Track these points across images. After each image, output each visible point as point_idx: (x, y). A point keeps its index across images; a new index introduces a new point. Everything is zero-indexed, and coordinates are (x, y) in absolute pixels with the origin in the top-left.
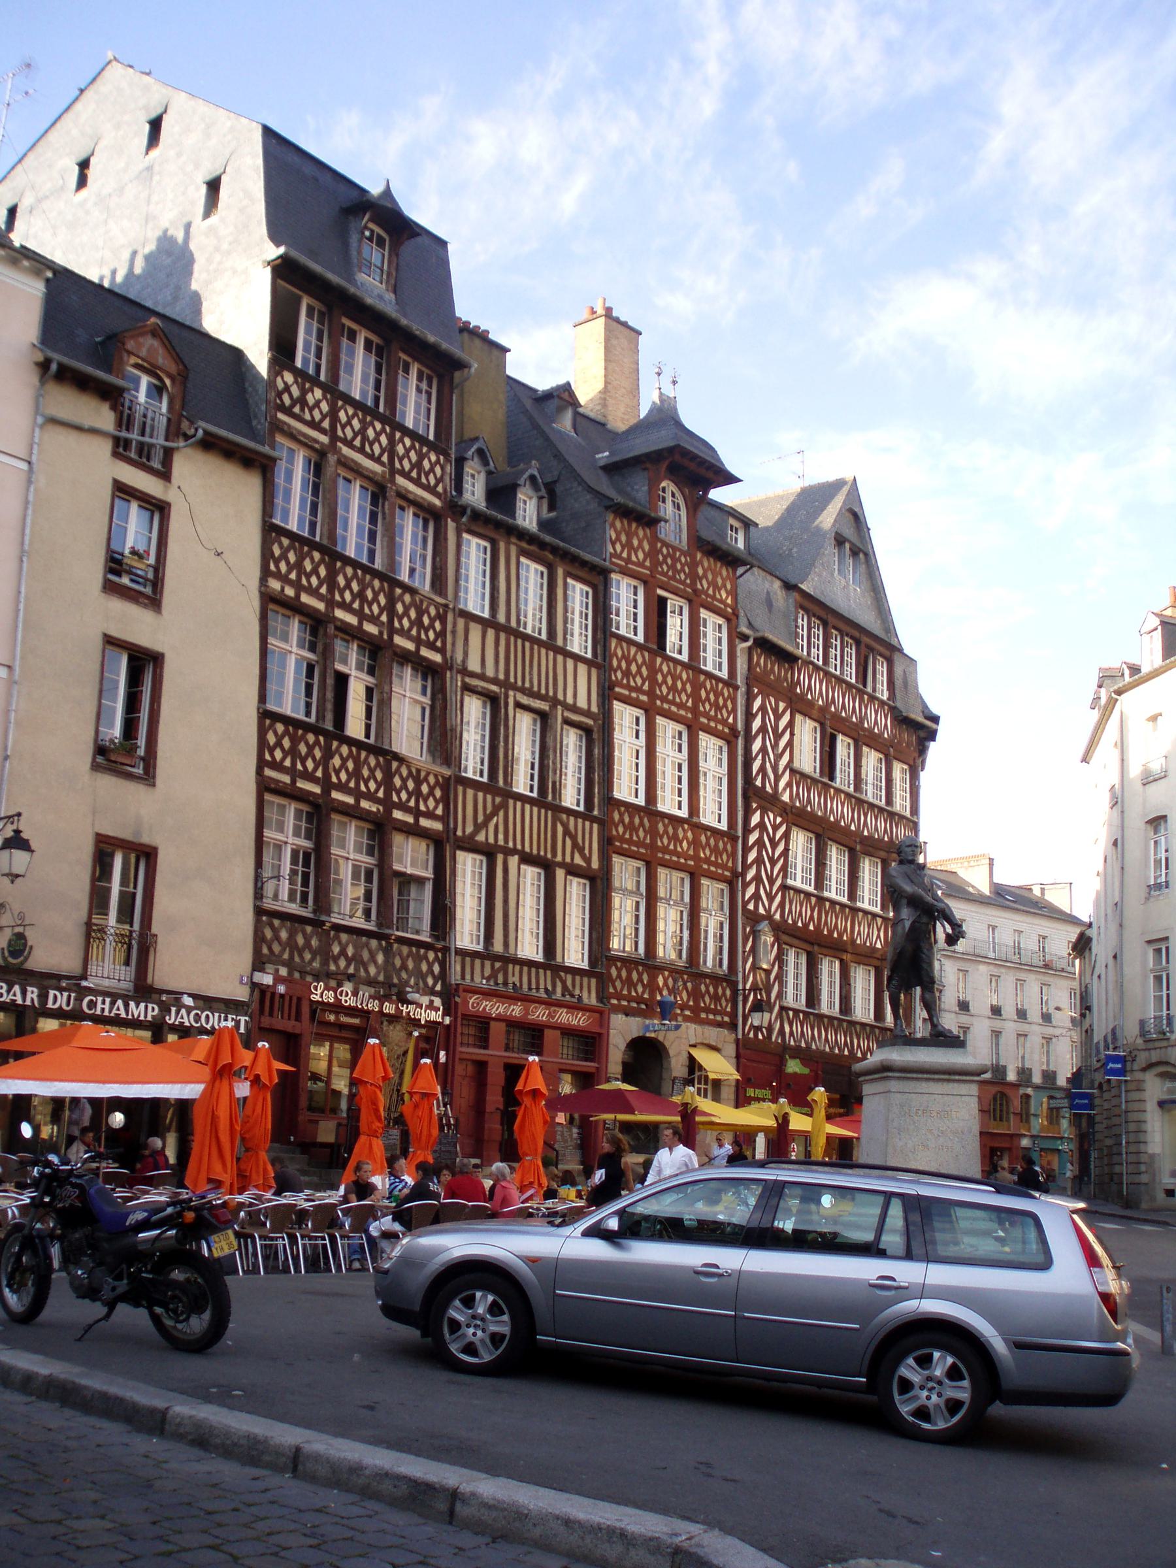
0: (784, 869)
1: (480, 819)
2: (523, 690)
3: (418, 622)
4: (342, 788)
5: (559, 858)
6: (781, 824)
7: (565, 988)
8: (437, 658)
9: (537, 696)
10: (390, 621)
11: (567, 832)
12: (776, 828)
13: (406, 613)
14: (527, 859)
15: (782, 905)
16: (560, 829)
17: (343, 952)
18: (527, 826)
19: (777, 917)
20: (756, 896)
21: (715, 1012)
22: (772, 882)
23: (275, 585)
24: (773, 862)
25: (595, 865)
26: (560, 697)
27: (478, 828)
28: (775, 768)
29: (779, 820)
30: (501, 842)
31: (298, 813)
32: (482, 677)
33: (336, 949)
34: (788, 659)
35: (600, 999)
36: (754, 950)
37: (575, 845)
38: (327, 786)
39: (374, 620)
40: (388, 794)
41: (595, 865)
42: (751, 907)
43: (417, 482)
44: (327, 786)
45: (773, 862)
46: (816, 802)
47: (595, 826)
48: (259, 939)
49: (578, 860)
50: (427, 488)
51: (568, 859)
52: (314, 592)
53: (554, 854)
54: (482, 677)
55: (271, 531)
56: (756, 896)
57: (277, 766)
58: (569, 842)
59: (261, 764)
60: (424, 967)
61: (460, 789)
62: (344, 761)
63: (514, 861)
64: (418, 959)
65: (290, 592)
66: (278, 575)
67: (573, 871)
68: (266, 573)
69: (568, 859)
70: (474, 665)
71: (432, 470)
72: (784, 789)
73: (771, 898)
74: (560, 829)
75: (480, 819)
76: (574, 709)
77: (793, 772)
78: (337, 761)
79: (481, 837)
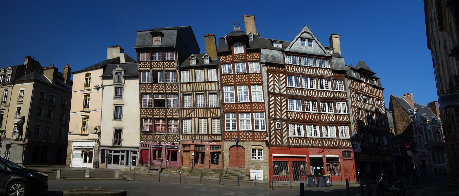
0: (287, 108)
1: (188, 113)
2: (197, 91)
3: (172, 87)
4: (156, 115)
5: (209, 116)
6: (283, 99)
7: (211, 138)
8: (177, 92)
9: (201, 91)
10: (165, 89)
11: (210, 111)
12: (281, 100)
13: (169, 87)
14: (199, 118)
15: (287, 115)
16: (209, 112)
17: (157, 137)
18: (200, 113)
19: (285, 118)
20: (275, 114)
21: (261, 138)
22: (281, 111)
23: (142, 91)
24: (281, 107)
25: (219, 115)
26: (207, 89)
27: (187, 115)
28: (279, 88)
29: (282, 98)
30: (193, 116)
31: (150, 120)
32: (187, 92)
33: (156, 137)
34: (283, 66)
35: (222, 138)
36: (275, 125)
37: (213, 113)
38: (153, 115)
39: (161, 90)
40: (166, 114)
41: (219, 115)
42: (273, 117)
43: (170, 67)
44: (153, 115)
45: (281, 107)
46: (298, 93)
47: (219, 109)
48: (141, 137)
49: (214, 116)
50: (172, 67)
51: (211, 116)
52: (149, 90)
53: (207, 115)
54: (187, 92)
55: (140, 84)
56: (275, 114)
57: (143, 115)
58: (211, 113)
59: (141, 115)
60: (175, 138)
61: (183, 110)
62: (157, 111)
63: (197, 119)
64: (173, 137)
65: (144, 91)
66: (142, 90)
67: (213, 118)
68: (140, 90)
69: (211, 116)
70: (185, 90)
71: (173, 64)
72: (284, 91)
73: (282, 115)
74: (209, 112)
75: (188, 113)
76: (211, 91)
77: (287, 88)
78: (155, 112)
79: (188, 116)
